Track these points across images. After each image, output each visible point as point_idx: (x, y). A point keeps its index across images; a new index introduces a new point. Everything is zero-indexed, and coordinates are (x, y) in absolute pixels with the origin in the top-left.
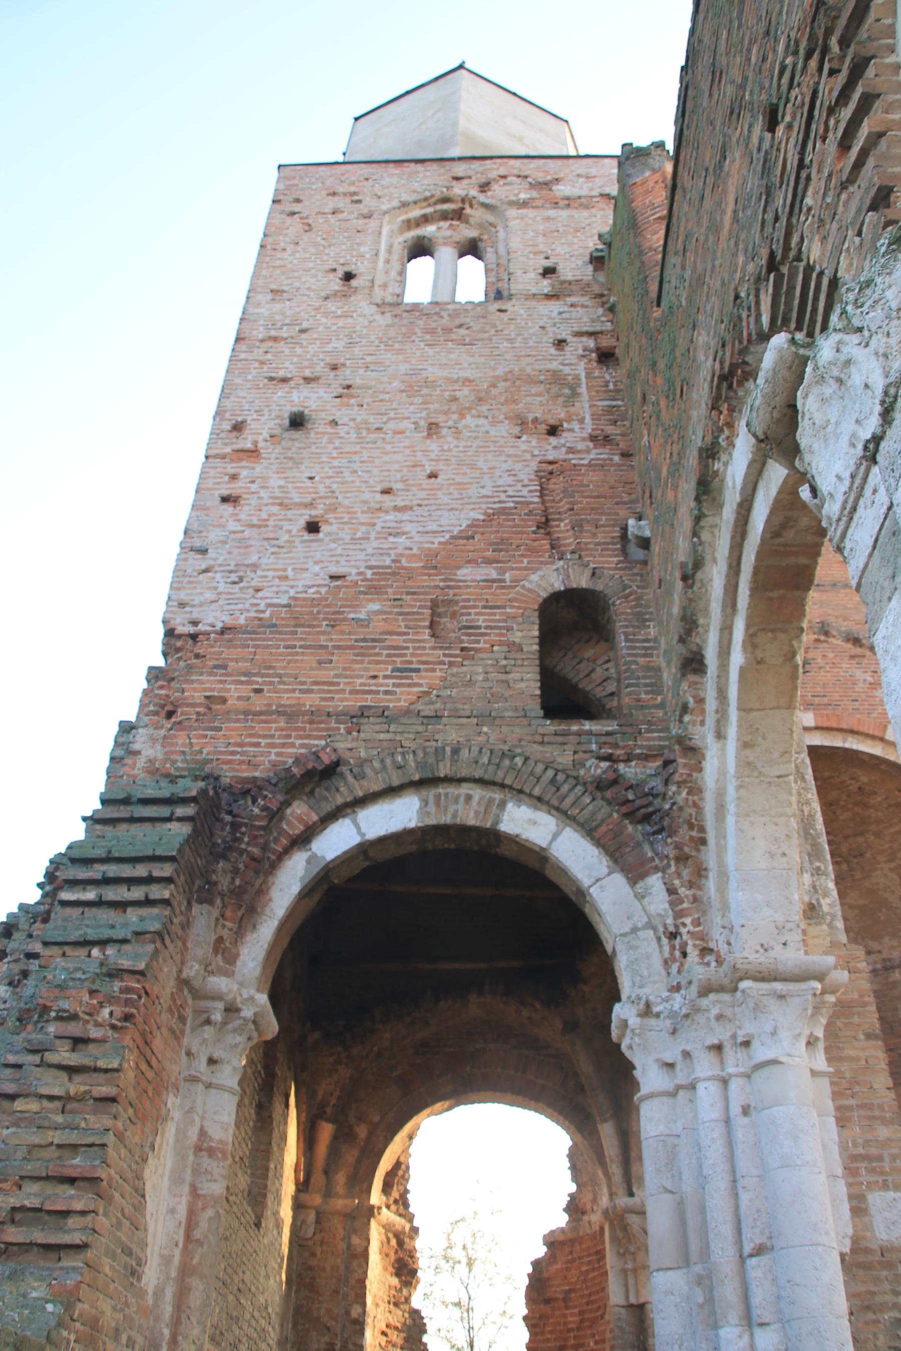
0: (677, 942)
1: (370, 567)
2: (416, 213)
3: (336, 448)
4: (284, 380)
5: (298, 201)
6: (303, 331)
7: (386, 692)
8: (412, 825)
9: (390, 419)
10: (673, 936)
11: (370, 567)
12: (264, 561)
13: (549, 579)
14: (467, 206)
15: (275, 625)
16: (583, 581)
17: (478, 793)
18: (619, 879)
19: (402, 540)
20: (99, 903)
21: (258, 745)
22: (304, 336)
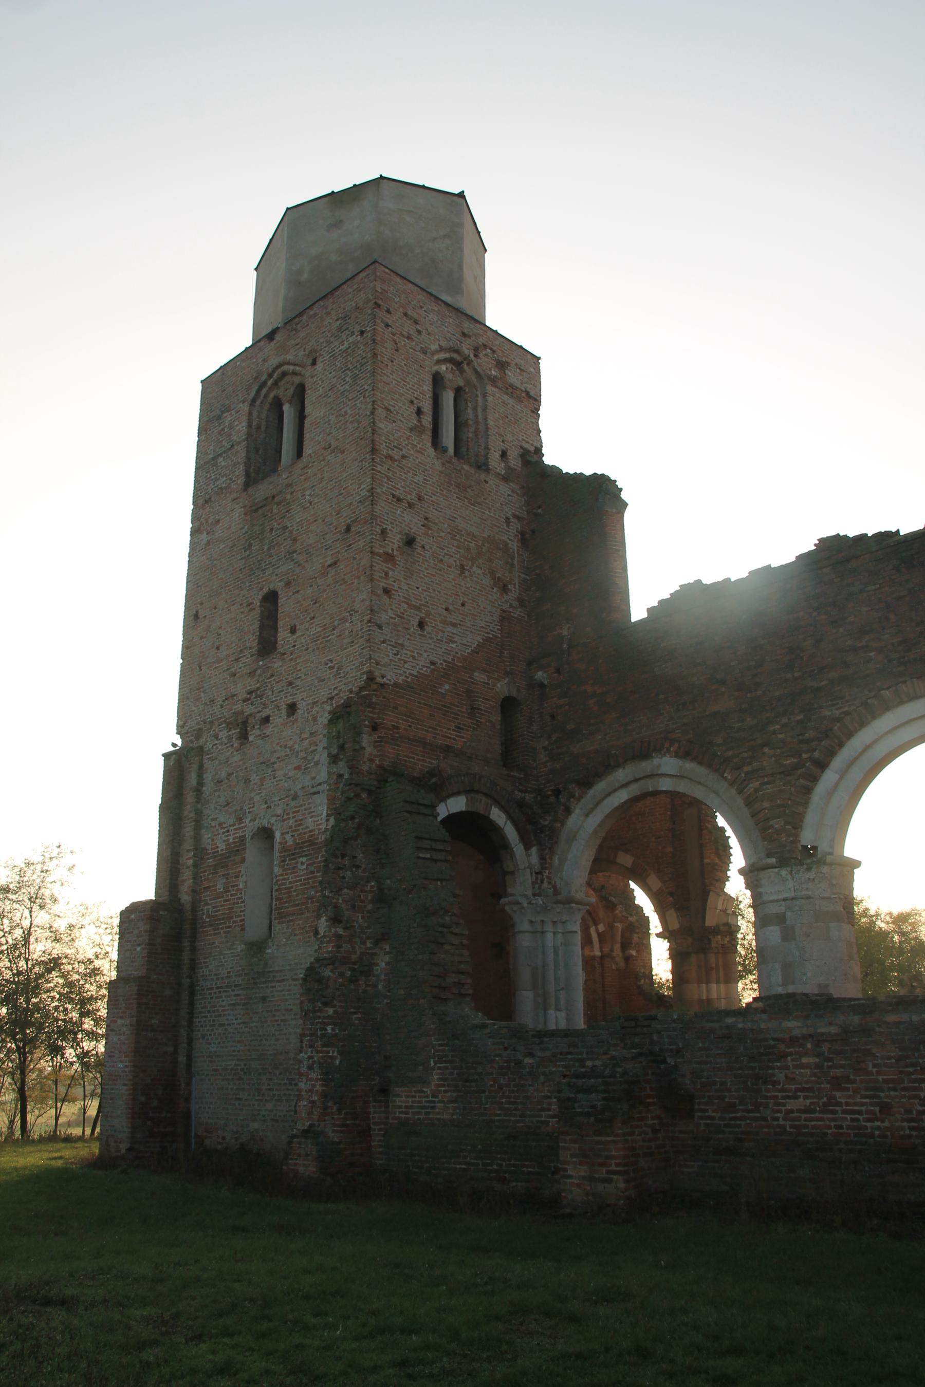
0: (539, 876)
1: (444, 661)
2: (442, 356)
3: (426, 569)
4: (399, 500)
5: (388, 311)
6: (403, 457)
7: (454, 739)
8: (464, 809)
9: (446, 554)
10: (537, 873)
11: (444, 661)
12: (406, 643)
13: (502, 688)
14: (465, 362)
15: (412, 688)
16: (514, 694)
17: (484, 799)
18: (521, 846)
19: (454, 646)
20: (431, 859)
21: (414, 758)
22: (404, 462)
